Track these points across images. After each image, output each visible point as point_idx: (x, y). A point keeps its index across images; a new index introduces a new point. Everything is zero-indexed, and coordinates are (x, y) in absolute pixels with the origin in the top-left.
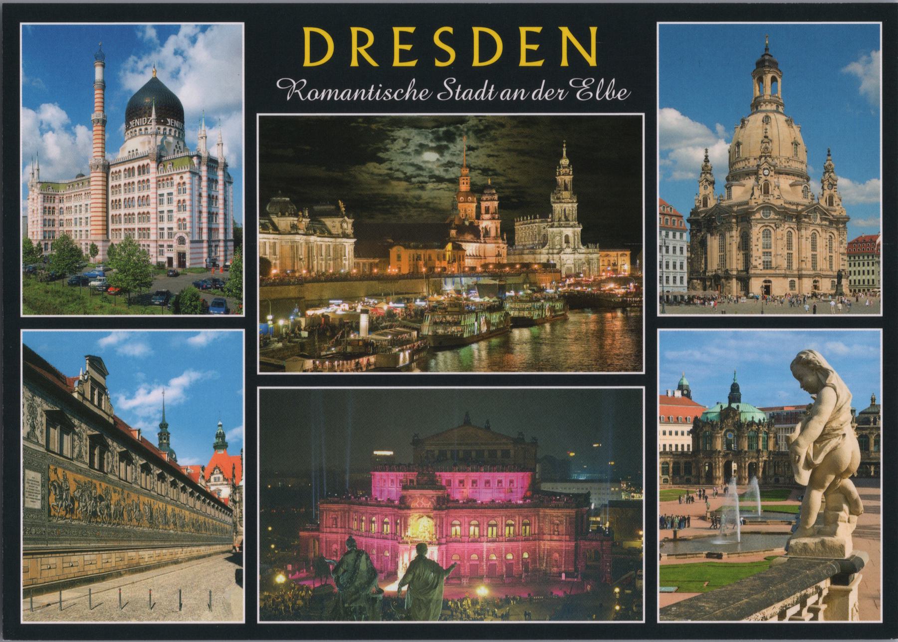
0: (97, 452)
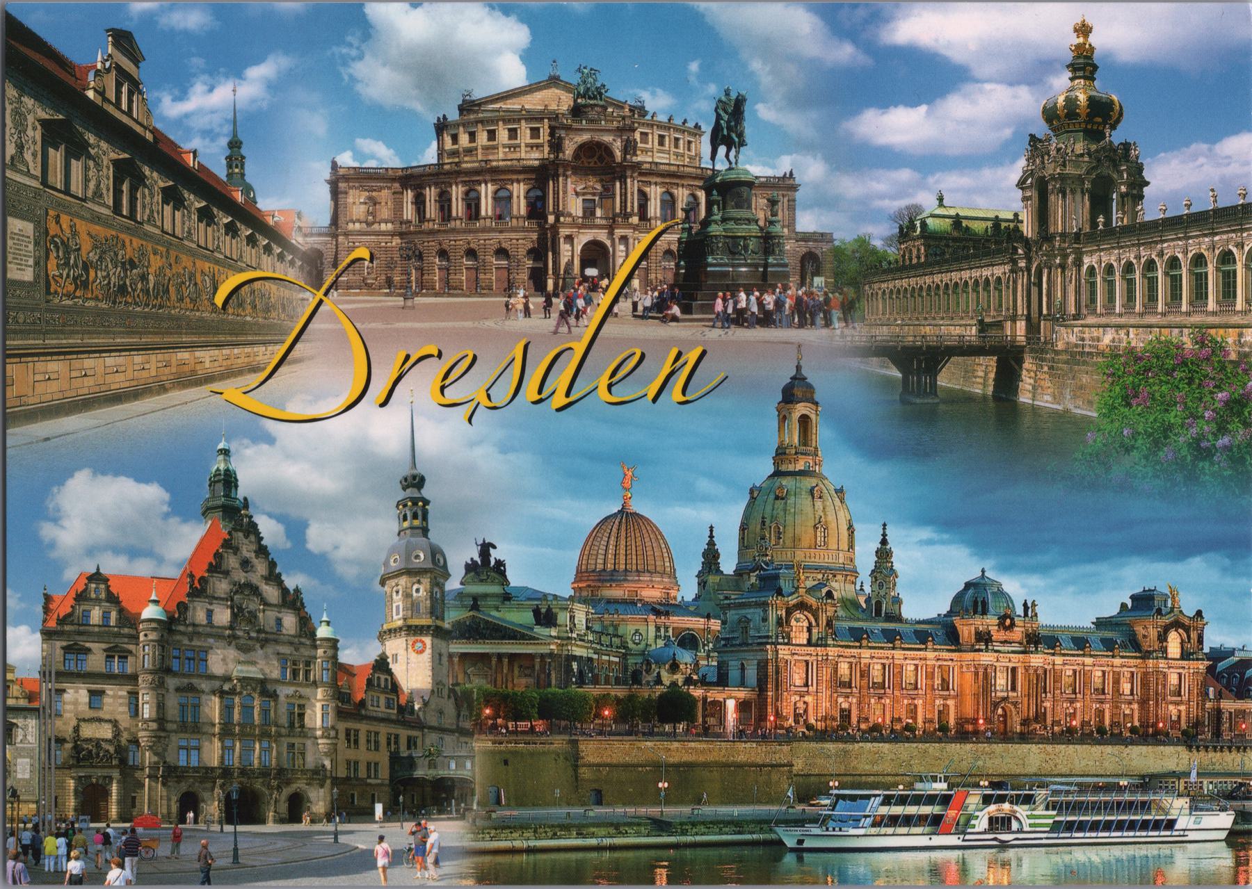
0: (125, 187)
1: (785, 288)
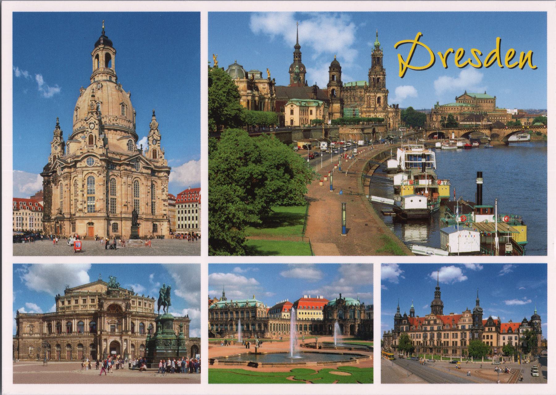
1: (185, 358)
